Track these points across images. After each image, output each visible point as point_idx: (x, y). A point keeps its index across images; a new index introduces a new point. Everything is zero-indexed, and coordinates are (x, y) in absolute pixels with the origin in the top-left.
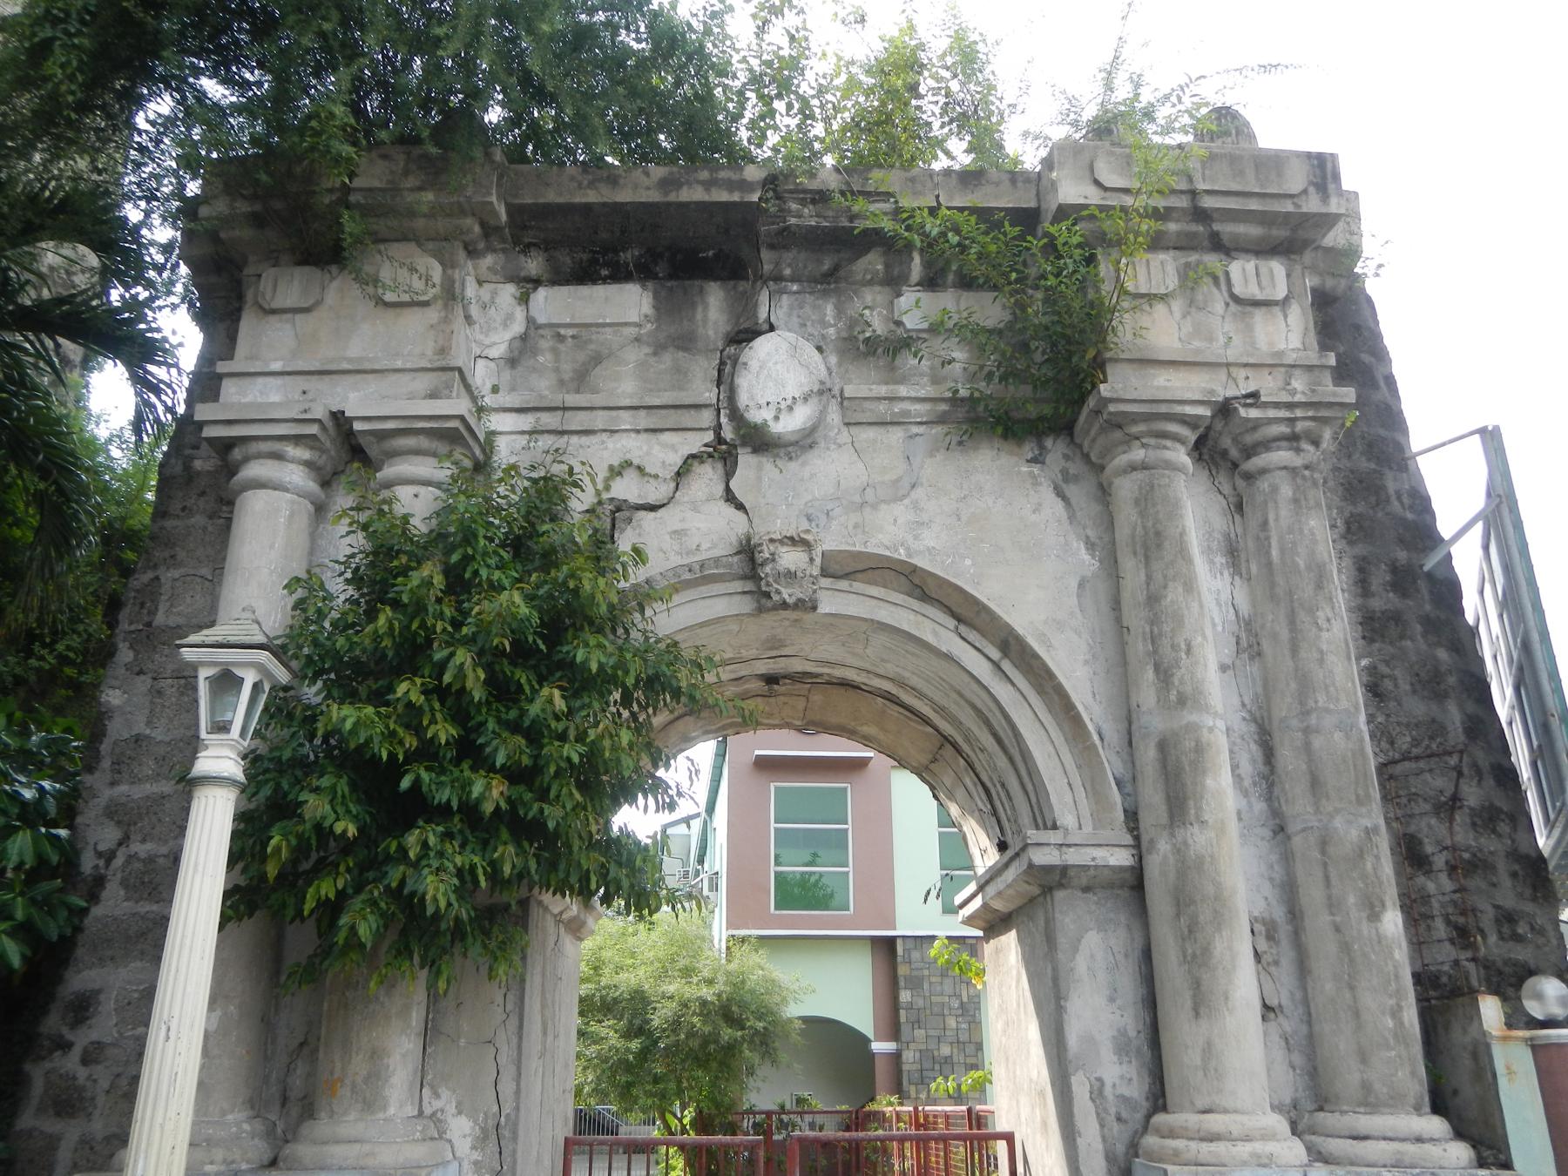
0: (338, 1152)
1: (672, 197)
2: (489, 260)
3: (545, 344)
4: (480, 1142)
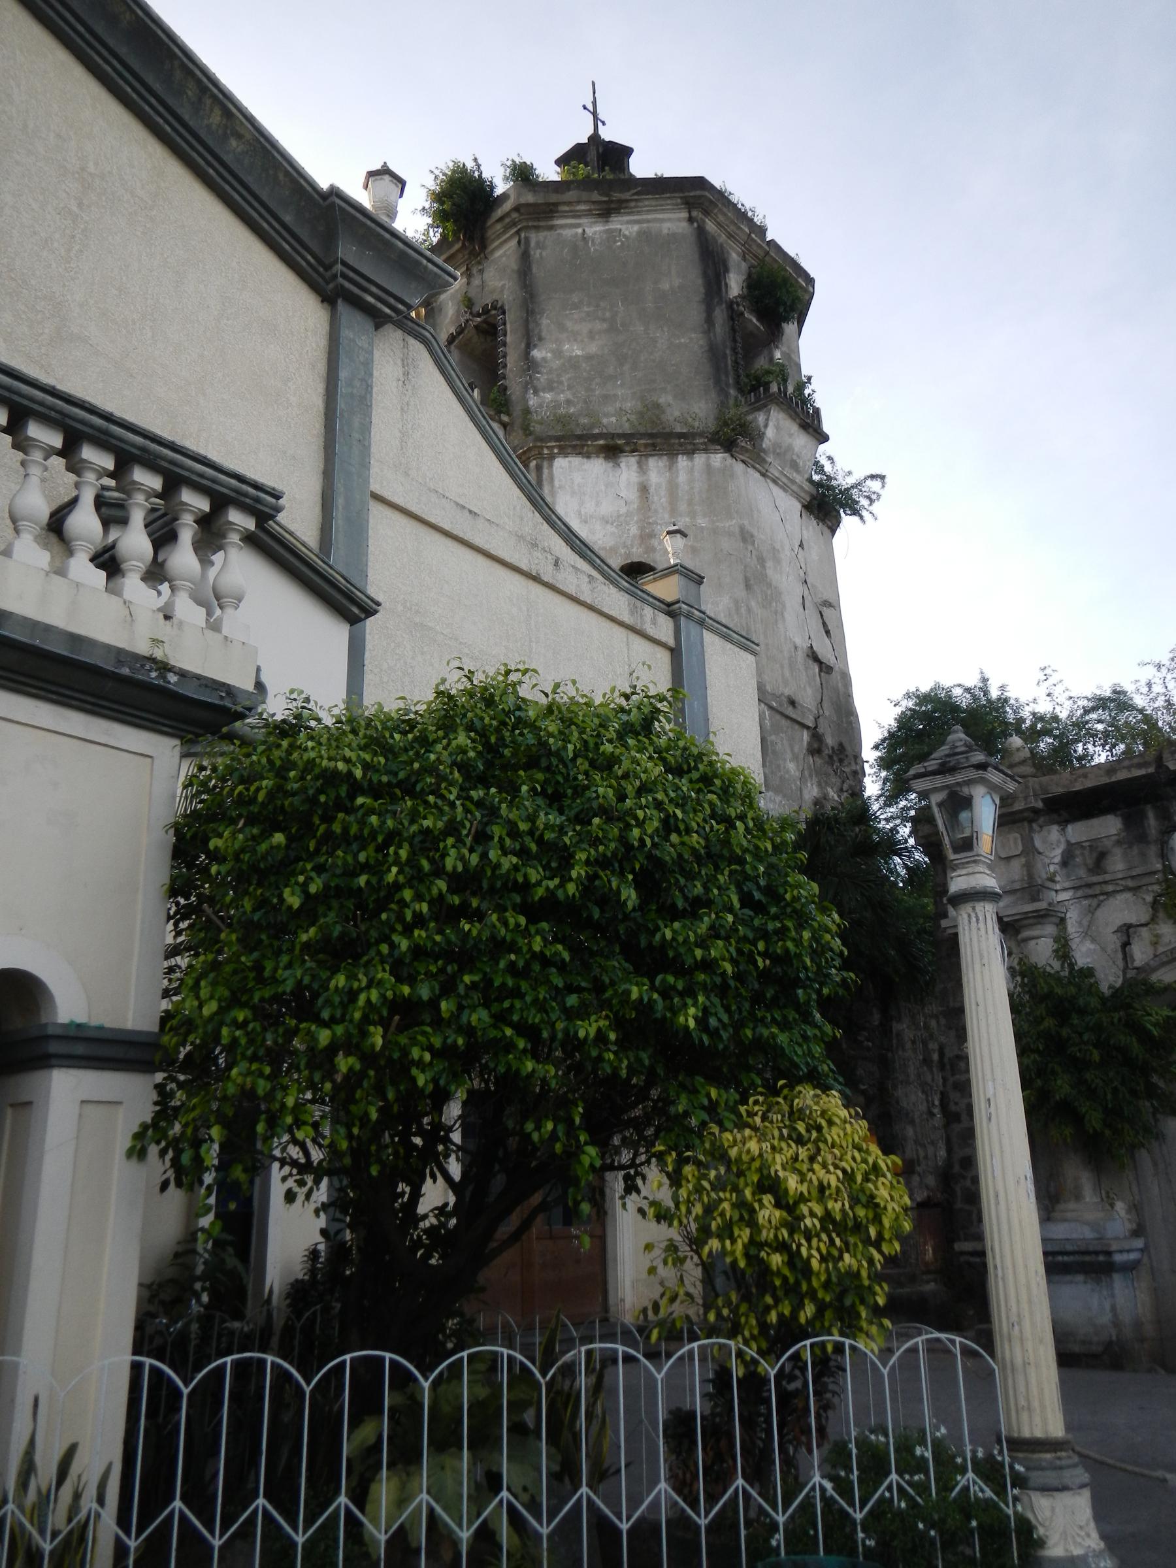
0: (1069, 1215)
1: (1114, 779)
2: (1041, 820)
3: (1078, 852)
4: (1128, 1211)
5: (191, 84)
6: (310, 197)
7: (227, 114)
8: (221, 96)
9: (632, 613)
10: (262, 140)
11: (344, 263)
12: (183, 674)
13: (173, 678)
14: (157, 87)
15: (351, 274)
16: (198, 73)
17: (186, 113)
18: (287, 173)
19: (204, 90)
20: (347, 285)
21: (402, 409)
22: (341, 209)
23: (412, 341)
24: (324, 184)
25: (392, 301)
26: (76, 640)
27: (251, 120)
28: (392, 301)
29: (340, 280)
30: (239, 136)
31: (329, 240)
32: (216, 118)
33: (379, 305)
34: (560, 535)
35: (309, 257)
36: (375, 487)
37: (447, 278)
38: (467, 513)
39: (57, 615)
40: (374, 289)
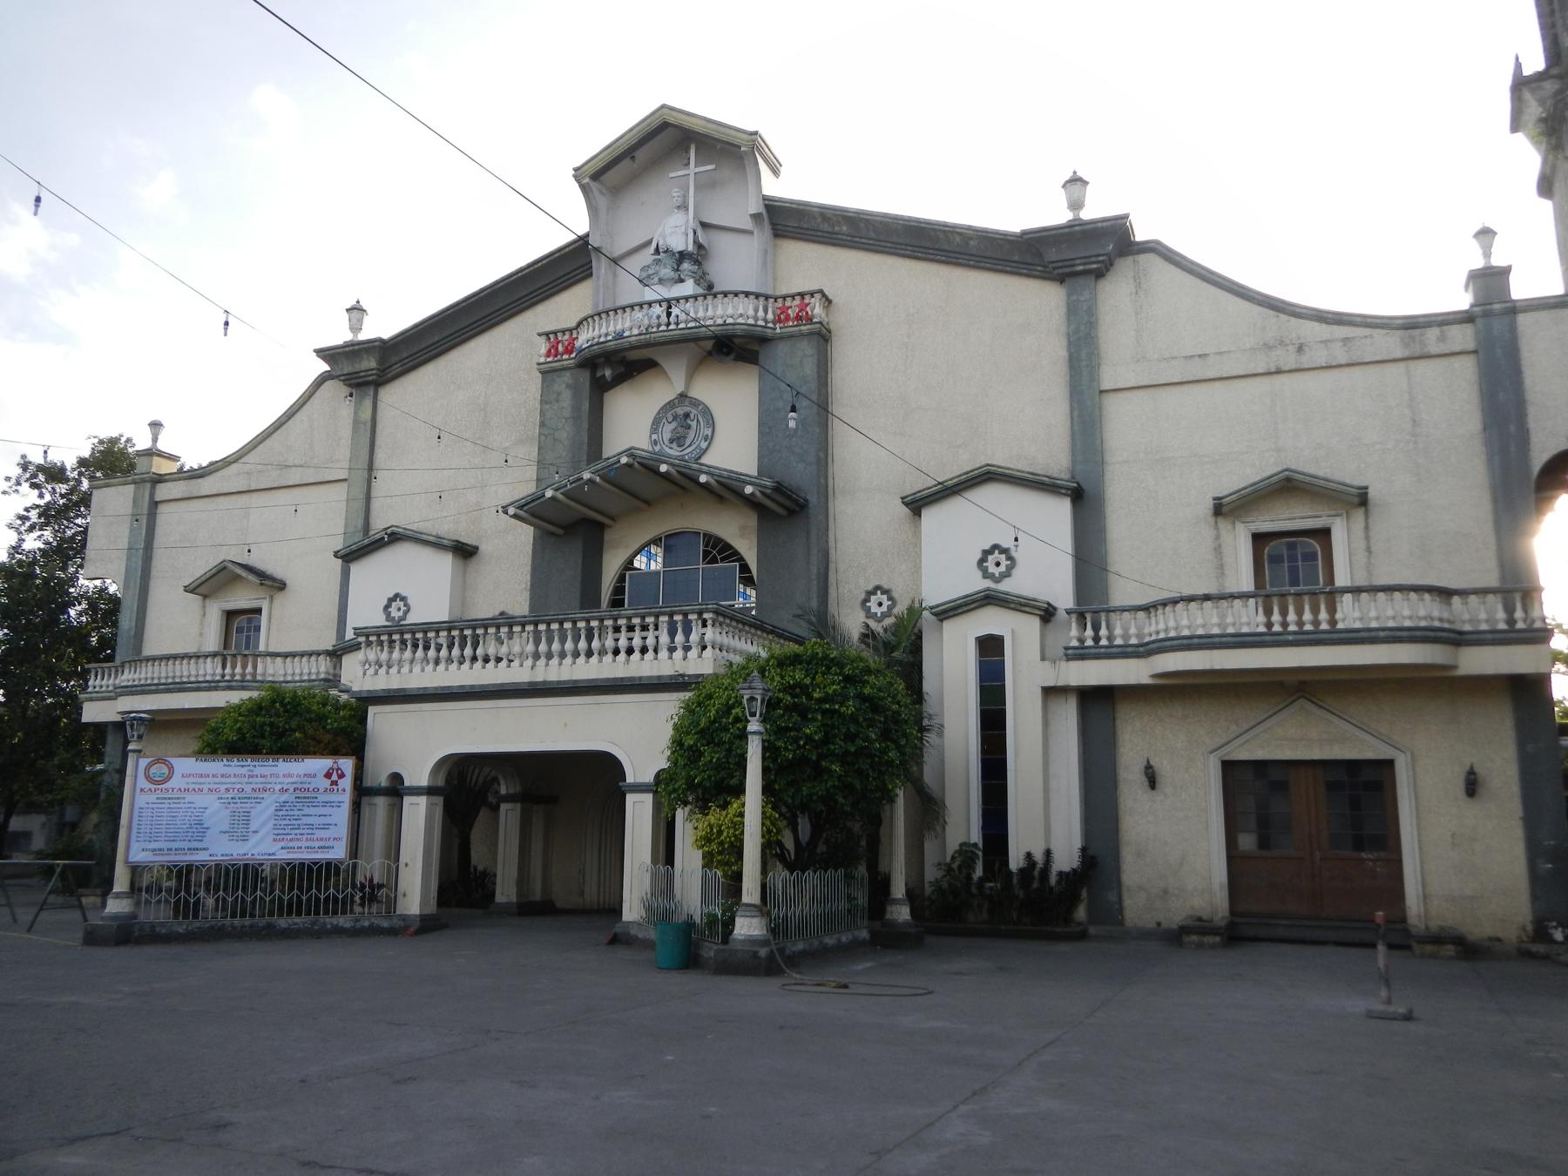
5: (939, 233)
6: (1017, 241)
7: (960, 234)
8: (951, 229)
9: (1407, 345)
10: (979, 234)
11: (1053, 262)
12: (689, 676)
13: (686, 678)
14: (928, 244)
15: (1060, 264)
16: (937, 227)
17: (946, 247)
18: (1001, 239)
19: (944, 231)
20: (1061, 271)
21: (1137, 313)
22: (1030, 238)
23: (1142, 258)
24: (1019, 231)
25: (1094, 259)
26: (659, 677)
27: (970, 228)
28: (1094, 259)
29: (1056, 271)
30: (971, 238)
31: (1040, 255)
32: (958, 239)
33: (1088, 267)
34: (1311, 320)
35: (1039, 268)
36: (1106, 385)
37: (1120, 221)
38: (1197, 359)
39: (655, 673)
40: (1078, 262)
